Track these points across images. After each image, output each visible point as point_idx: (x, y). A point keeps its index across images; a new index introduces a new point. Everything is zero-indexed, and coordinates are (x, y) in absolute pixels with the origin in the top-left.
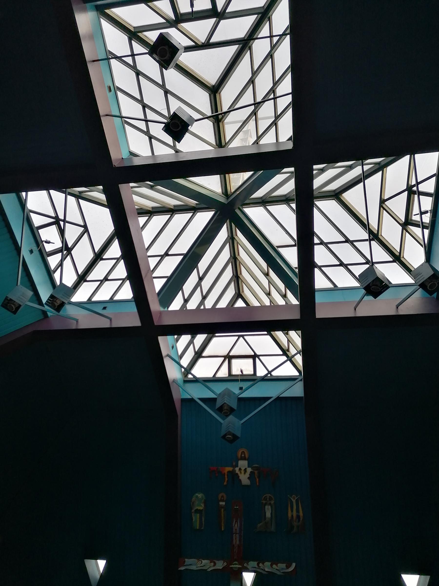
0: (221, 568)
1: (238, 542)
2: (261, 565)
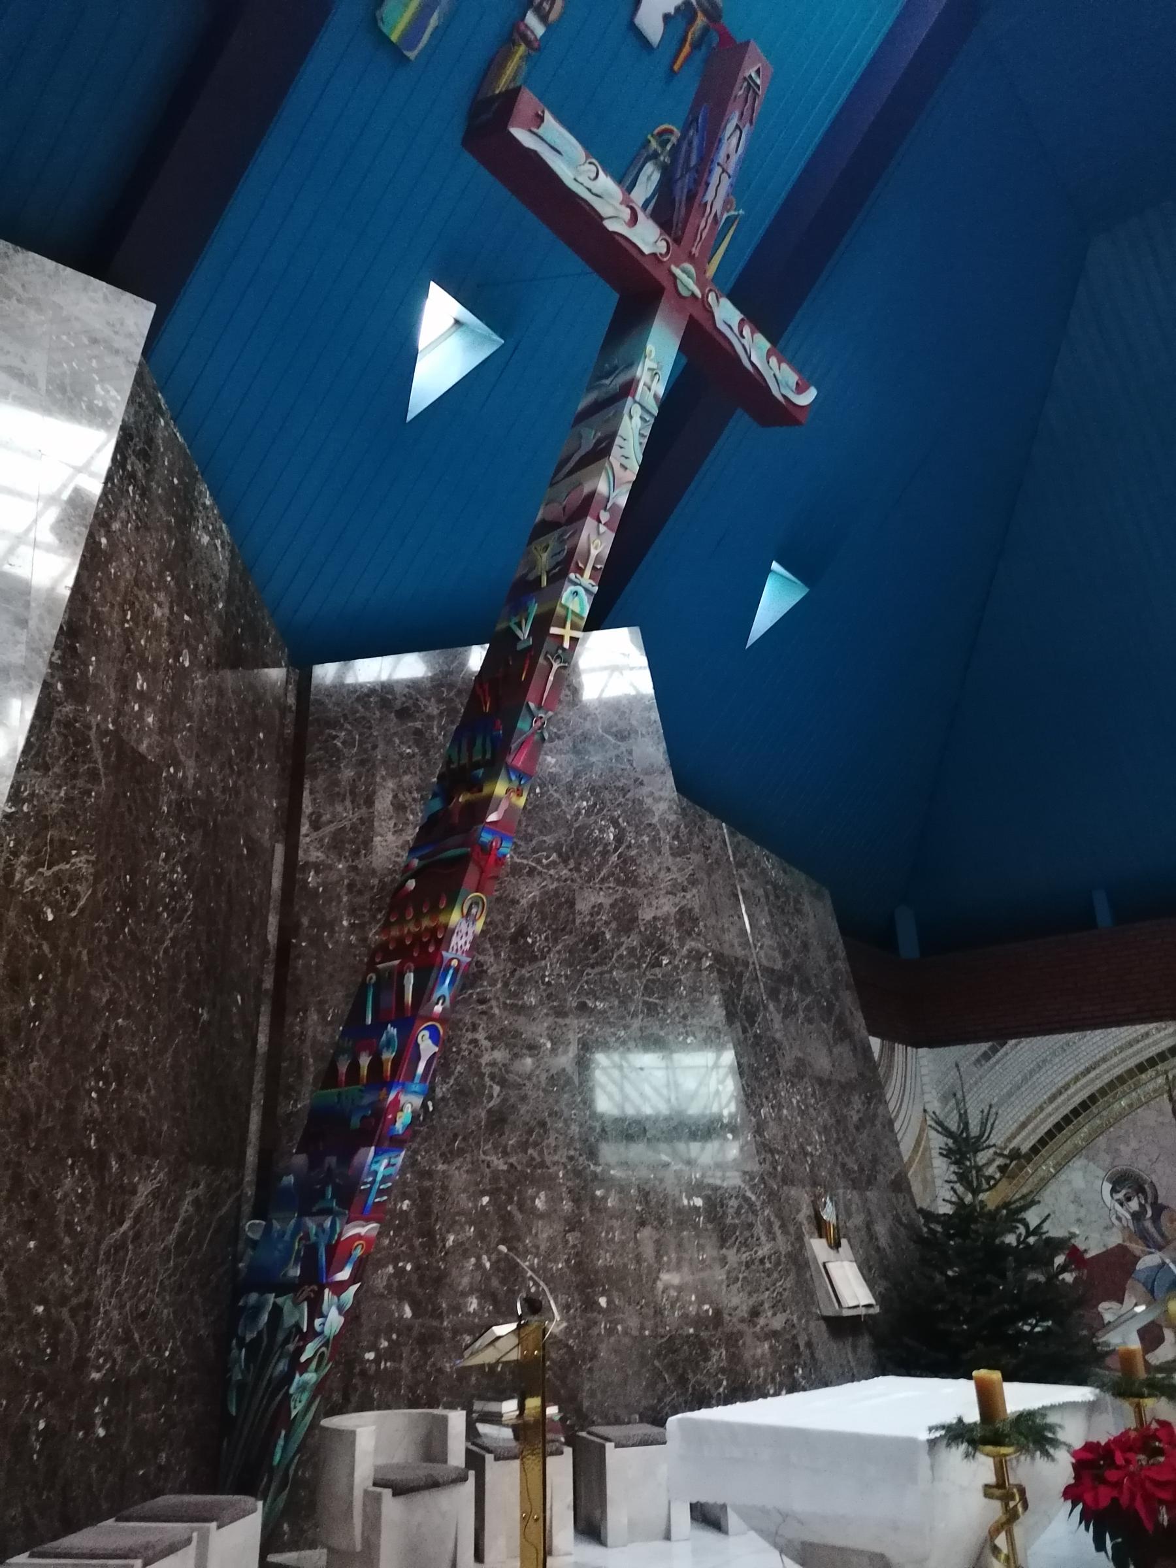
2: (747, 331)
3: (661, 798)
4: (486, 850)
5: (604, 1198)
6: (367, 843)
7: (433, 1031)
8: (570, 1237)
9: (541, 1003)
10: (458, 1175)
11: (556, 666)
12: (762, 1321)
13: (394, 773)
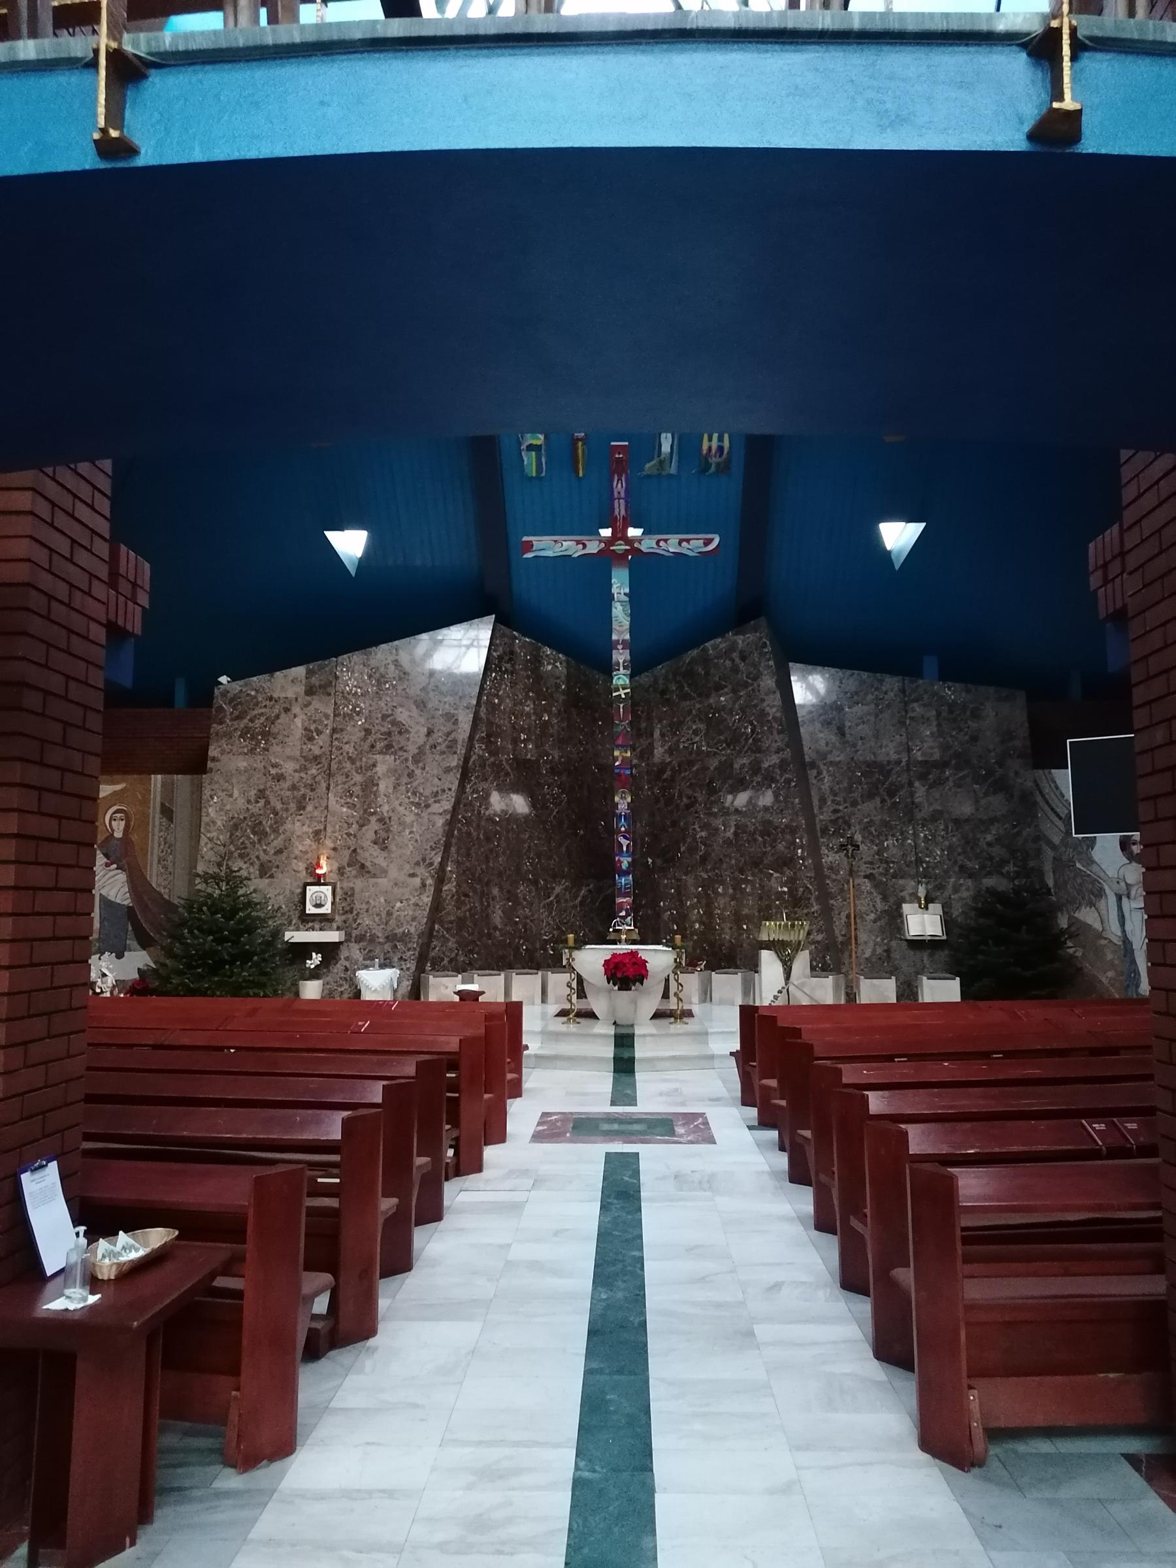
0: (595, 552)
1: (623, 512)
3: (774, 706)
4: (619, 775)
5: (745, 889)
6: (652, 753)
7: (625, 838)
8: (732, 903)
9: (719, 810)
10: (689, 880)
11: (622, 705)
12: (812, 937)
13: (660, 721)
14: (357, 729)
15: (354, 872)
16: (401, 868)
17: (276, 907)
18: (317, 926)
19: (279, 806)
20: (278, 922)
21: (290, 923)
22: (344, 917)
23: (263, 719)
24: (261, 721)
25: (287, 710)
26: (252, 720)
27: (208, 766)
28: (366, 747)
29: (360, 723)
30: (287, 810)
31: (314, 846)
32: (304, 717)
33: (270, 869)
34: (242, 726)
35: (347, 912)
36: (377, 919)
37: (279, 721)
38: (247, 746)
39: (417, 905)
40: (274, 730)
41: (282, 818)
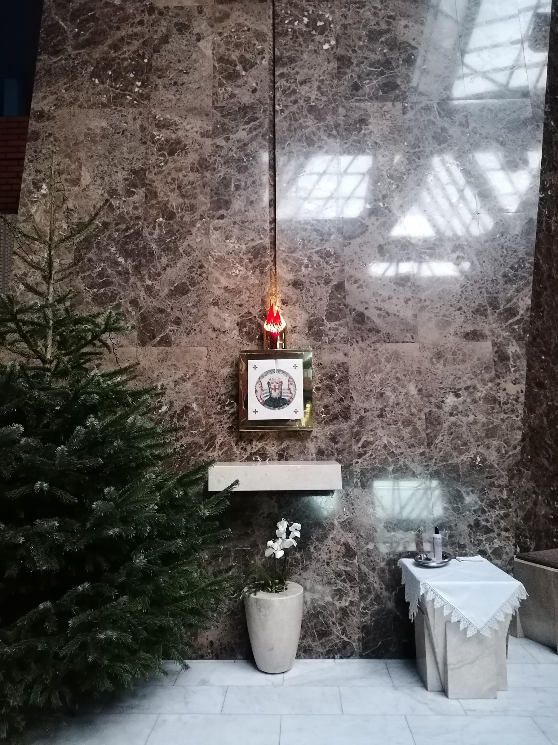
14: (320, 59)
15: (343, 331)
16: (445, 323)
17: (177, 408)
18: (272, 449)
19: (175, 200)
20: (184, 441)
21: (211, 442)
22: (330, 429)
23: (136, 44)
24: (133, 49)
25: (182, 28)
26: (115, 47)
27: (31, 128)
28: (344, 87)
29: (326, 46)
30: (192, 208)
31: (253, 280)
32: (218, 39)
33: (163, 327)
34: (97, 55)
35: (335, 417)
36: (406, 432)
37: (169, 47)
38: (106, 92)
39: (495, 400)
40: (159, 61)
41: (182, 224)
